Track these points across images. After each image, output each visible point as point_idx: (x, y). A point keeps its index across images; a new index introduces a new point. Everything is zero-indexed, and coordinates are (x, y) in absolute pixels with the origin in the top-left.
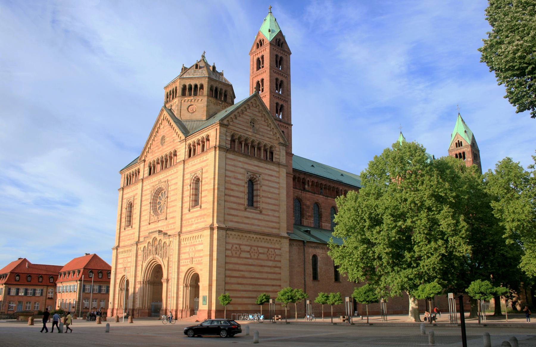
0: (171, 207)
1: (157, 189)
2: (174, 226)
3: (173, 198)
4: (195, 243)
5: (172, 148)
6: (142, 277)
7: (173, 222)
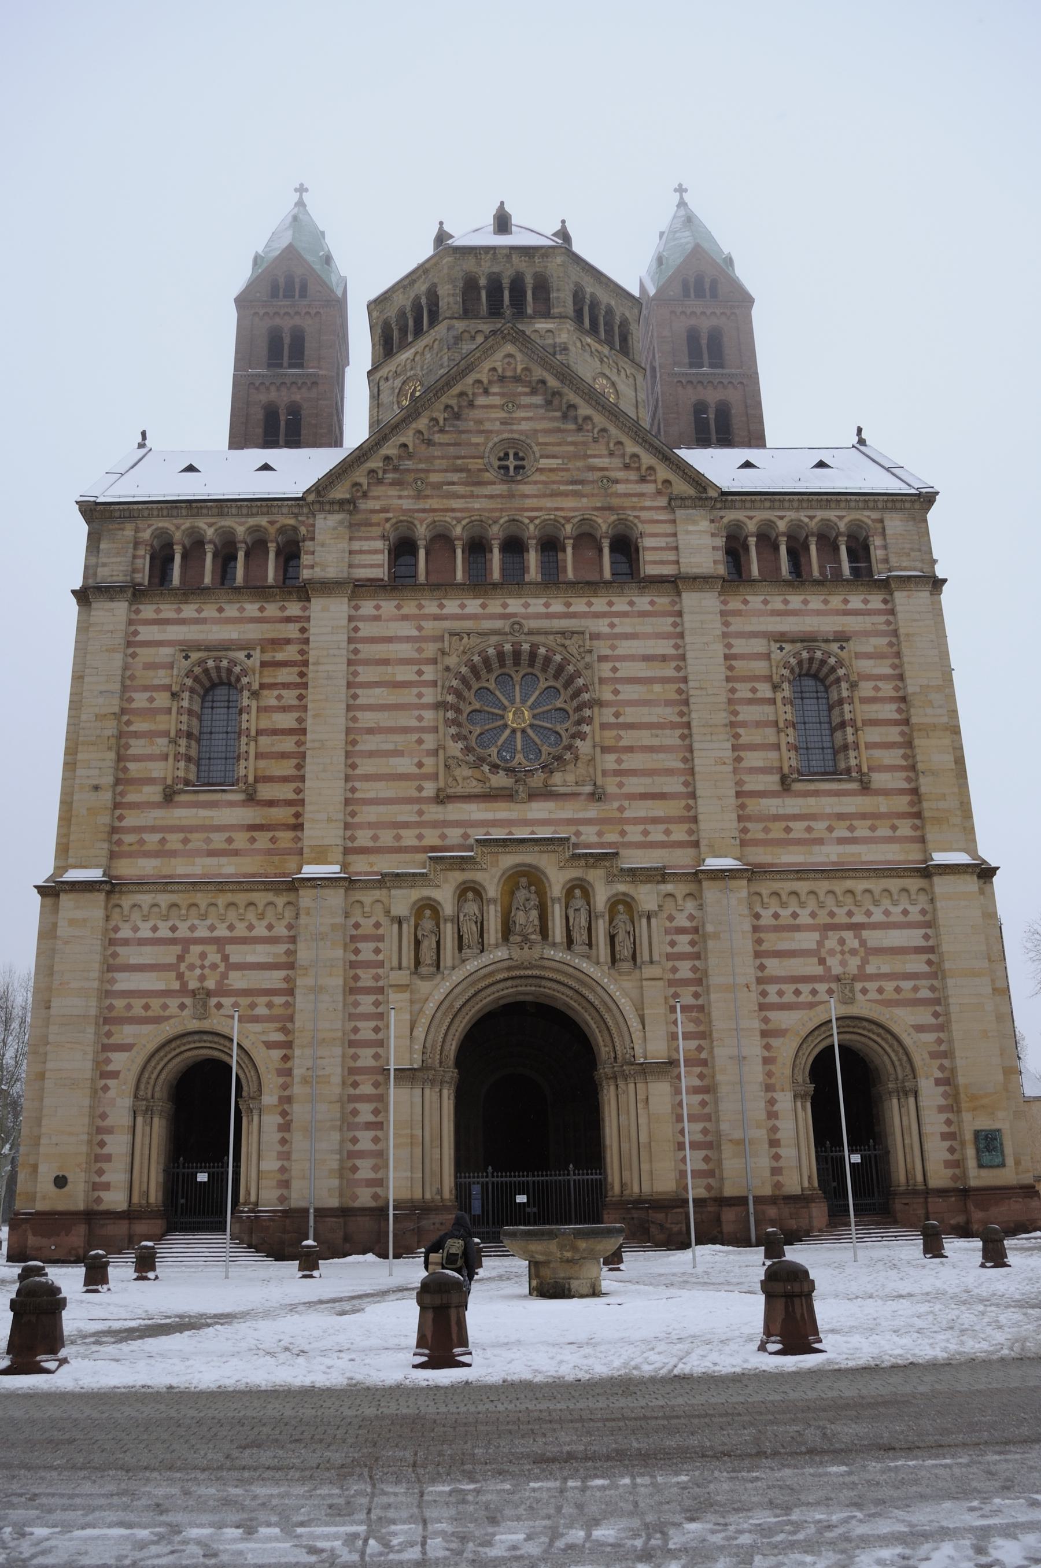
0: (630, 749)
1: (491, 651)
2: (667, 832)
3: (631, 715)
4: (859, 918)
5: (597, 509)
6: (418, 1047)
7: (660, 813)
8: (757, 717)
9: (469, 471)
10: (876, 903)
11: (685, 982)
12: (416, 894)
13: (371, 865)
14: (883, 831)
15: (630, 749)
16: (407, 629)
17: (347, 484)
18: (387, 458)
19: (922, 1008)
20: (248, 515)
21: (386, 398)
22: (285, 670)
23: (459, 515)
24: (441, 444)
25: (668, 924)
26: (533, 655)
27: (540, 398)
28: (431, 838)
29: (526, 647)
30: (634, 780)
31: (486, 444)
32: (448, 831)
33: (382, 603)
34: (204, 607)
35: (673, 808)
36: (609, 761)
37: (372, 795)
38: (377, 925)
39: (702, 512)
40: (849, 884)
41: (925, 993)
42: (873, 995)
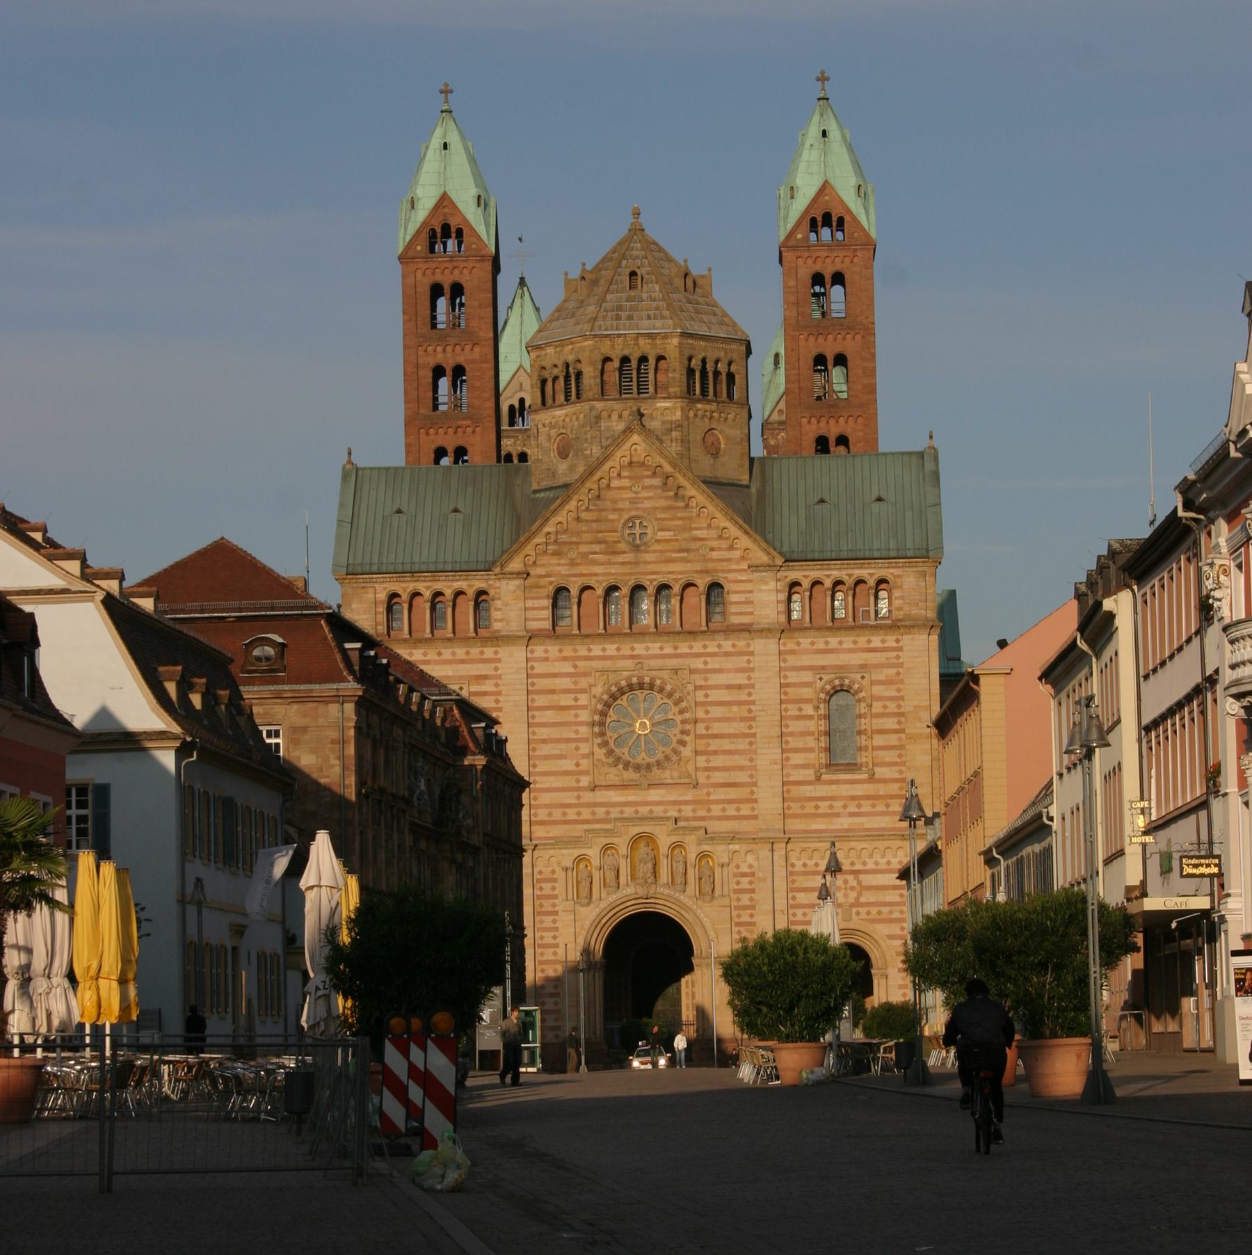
0: (715, 753)
1: (623, 683)
2: (738, 810)
3: (717, 728)
4: (858, 867)
5: (697, 572)
7: (735, 797)
8: (801, 729)
9: (606, 542)
10: (871, 856)
11: (745, 908)
12: (576, 853)
13: (548, 832)
14: (880, 808)
15: (715, 753)
16: (567, 668)
17: (521, 556)
18: (549, 533)
19: (893, 925)
20: (453, 580)
21: (542, 439)
22: (486, 698)
23: (601, 578)
24: (587, 521)
25: (735, 871)
26: (651, 686)
27: (658, 480)
28: (586, 814)
29: (647, 680)
30: (717, 774)
31: (619, 520)
32: (597, 810)
33: (549, 648)
34: (428, 651)
35: (743, 793)
36: (701, 761)
37: (547, 785)
38: (553, 872)
39: (771, 574)
40: (853, 844)
41: (896, 915)
42: (863, 916)
